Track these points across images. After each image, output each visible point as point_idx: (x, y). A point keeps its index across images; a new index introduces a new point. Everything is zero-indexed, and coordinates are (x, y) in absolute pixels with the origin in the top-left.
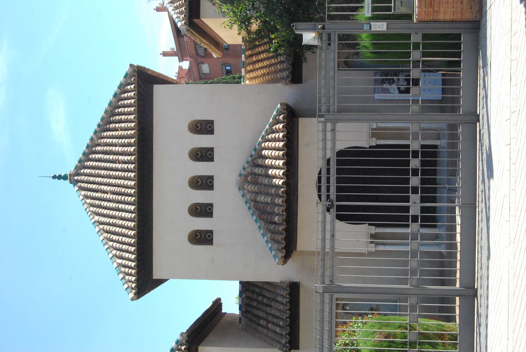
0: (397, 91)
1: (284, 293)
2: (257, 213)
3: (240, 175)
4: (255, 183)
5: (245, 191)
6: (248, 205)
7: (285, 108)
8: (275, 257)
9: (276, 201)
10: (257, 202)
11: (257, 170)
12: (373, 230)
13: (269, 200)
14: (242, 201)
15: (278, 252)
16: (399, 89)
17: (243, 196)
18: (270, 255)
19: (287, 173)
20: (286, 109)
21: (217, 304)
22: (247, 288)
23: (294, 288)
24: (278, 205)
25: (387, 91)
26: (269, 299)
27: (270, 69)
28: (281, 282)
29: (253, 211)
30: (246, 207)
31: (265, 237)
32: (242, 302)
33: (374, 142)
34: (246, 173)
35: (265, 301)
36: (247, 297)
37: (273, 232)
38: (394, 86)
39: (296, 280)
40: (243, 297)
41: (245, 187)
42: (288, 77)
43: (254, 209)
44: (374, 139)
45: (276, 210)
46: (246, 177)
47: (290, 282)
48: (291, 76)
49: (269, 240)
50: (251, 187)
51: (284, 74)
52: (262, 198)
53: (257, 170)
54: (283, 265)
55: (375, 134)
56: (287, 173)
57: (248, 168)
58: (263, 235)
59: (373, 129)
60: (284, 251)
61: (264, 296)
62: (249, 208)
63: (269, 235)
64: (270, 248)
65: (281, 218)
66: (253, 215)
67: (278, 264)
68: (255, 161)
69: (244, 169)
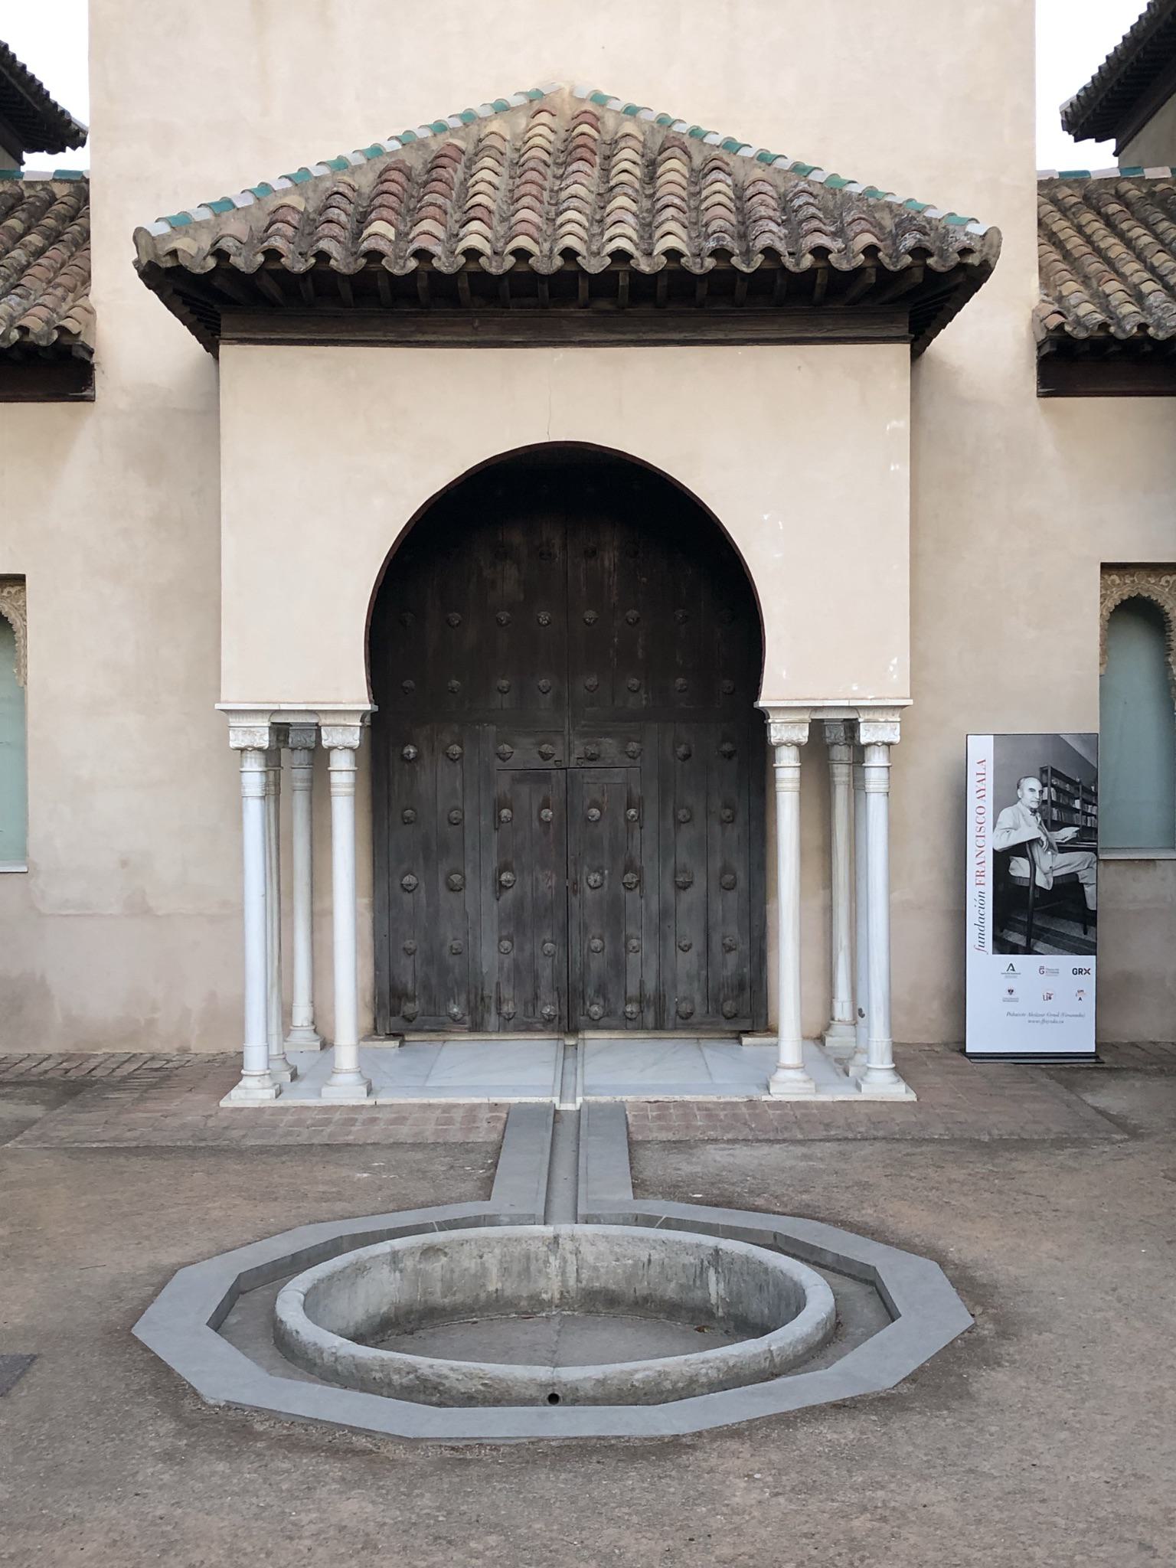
0: (1004, 842)
1: (34, 323)
2: (416, 162)
3: (599, 99)
4: (569, 151)
5: (522, 122)
6: (457, 123)
7: (973, 260)
8: (181, 224)
9: (475, 225)
10: (471, 163)
11: (627, 157)
12: (345, 738)
13: (478, 199)
14: (478, 101)
15: (206, 244)
16: (1021, 850)
17: (501, 108)
18: (191, 203)
19: (623, 281)
20: (961, 267)
21: (60, 133)
22: (79, 185)
23: (57, 369)
24: (456, 237)
25: (1005, 798)
26: (22, 270)
27: (1090, 259)
28: (90, 311)
29: (423, 144)
30: (447, 111)
31: (288, 184)
32: (31, 184)
33: (786, 733)
34: (610, 122)
35: (18, 255)
36: (53, 199)
37: (310, 225)
38: (1029, 829)
39: (102, 383)
40: (61, 190)
41: (544, 117)
42: (1078, 322)
43: (435, 146)
44: (803, 735)
45: (427, 225)
46: (595, 121)
47: (91, 352)
48: (1083, 335)
49: (273, 203)
50: (544, 134)
51: (1085, 308)
52: (488, 176)
53: (627, 157)
54: (137, 263)
55: (834, 741)
56: (623, 281)
57: (639, 124)
58: (300, 180)
59: (852, 726)
60: (211, 263)
61: (40, 253)
62: (440, 128)
63: (295, 200)
64: (227, 204)
65: (383, 246)
66: (407, 140)
67: (139, 235)
68: (678, 152)
69: (631, 111)
